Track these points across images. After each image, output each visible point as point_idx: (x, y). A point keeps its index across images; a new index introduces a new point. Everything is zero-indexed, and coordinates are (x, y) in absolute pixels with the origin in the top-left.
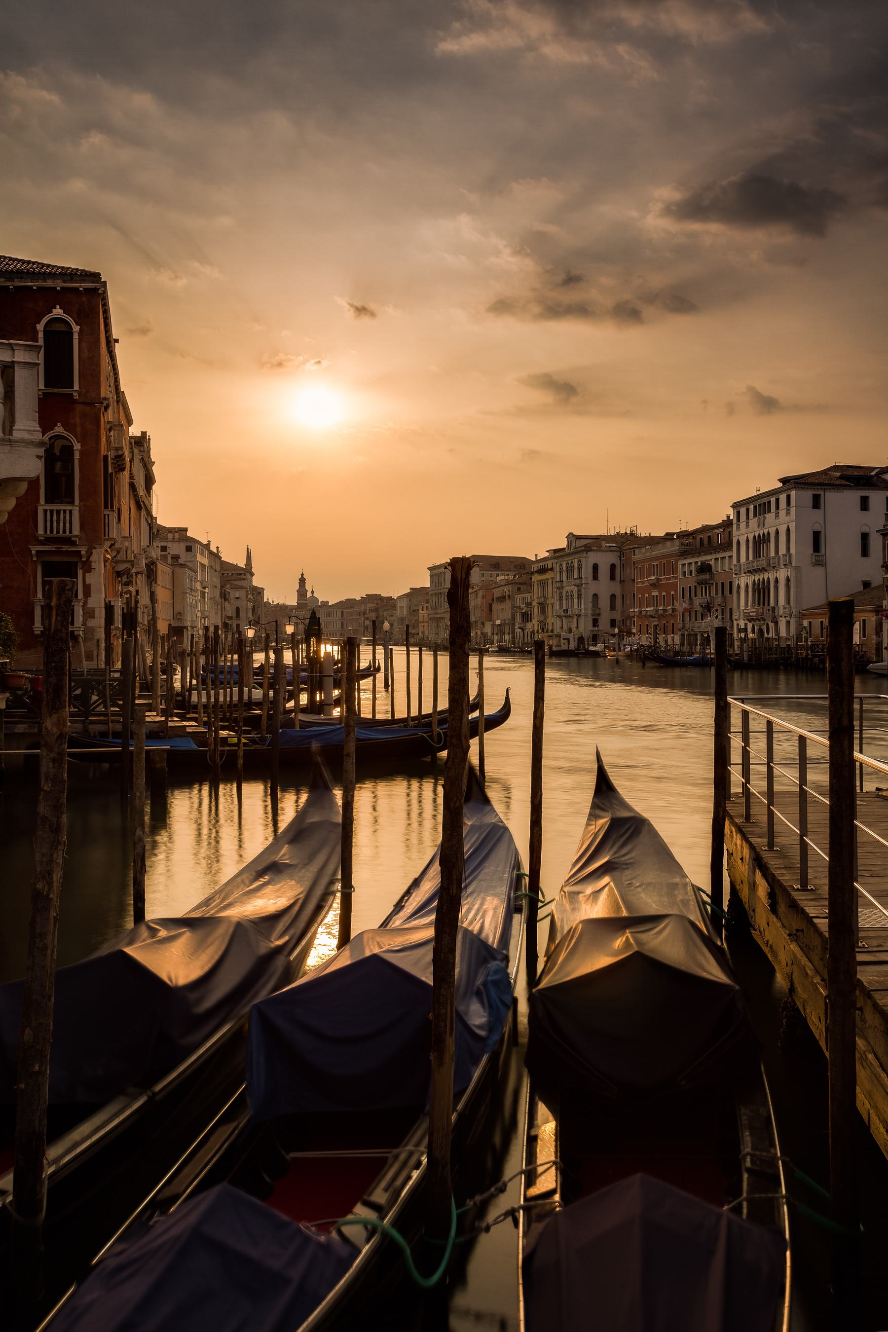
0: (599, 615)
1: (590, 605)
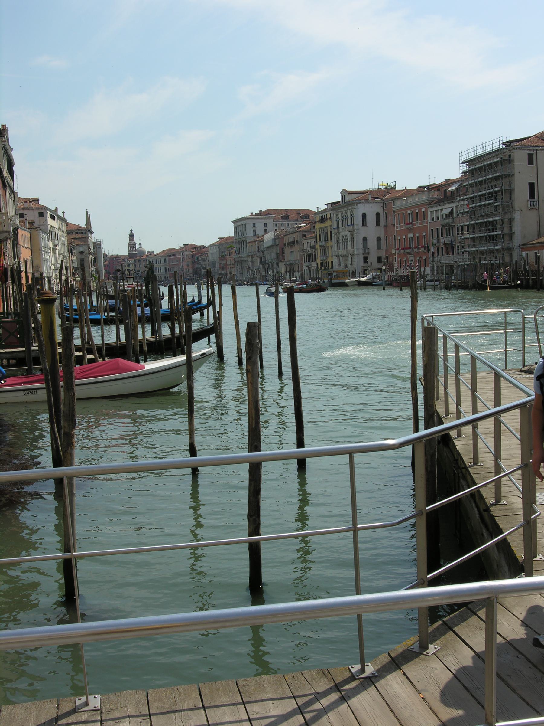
0: (368, 253)
1: (361, 246)
